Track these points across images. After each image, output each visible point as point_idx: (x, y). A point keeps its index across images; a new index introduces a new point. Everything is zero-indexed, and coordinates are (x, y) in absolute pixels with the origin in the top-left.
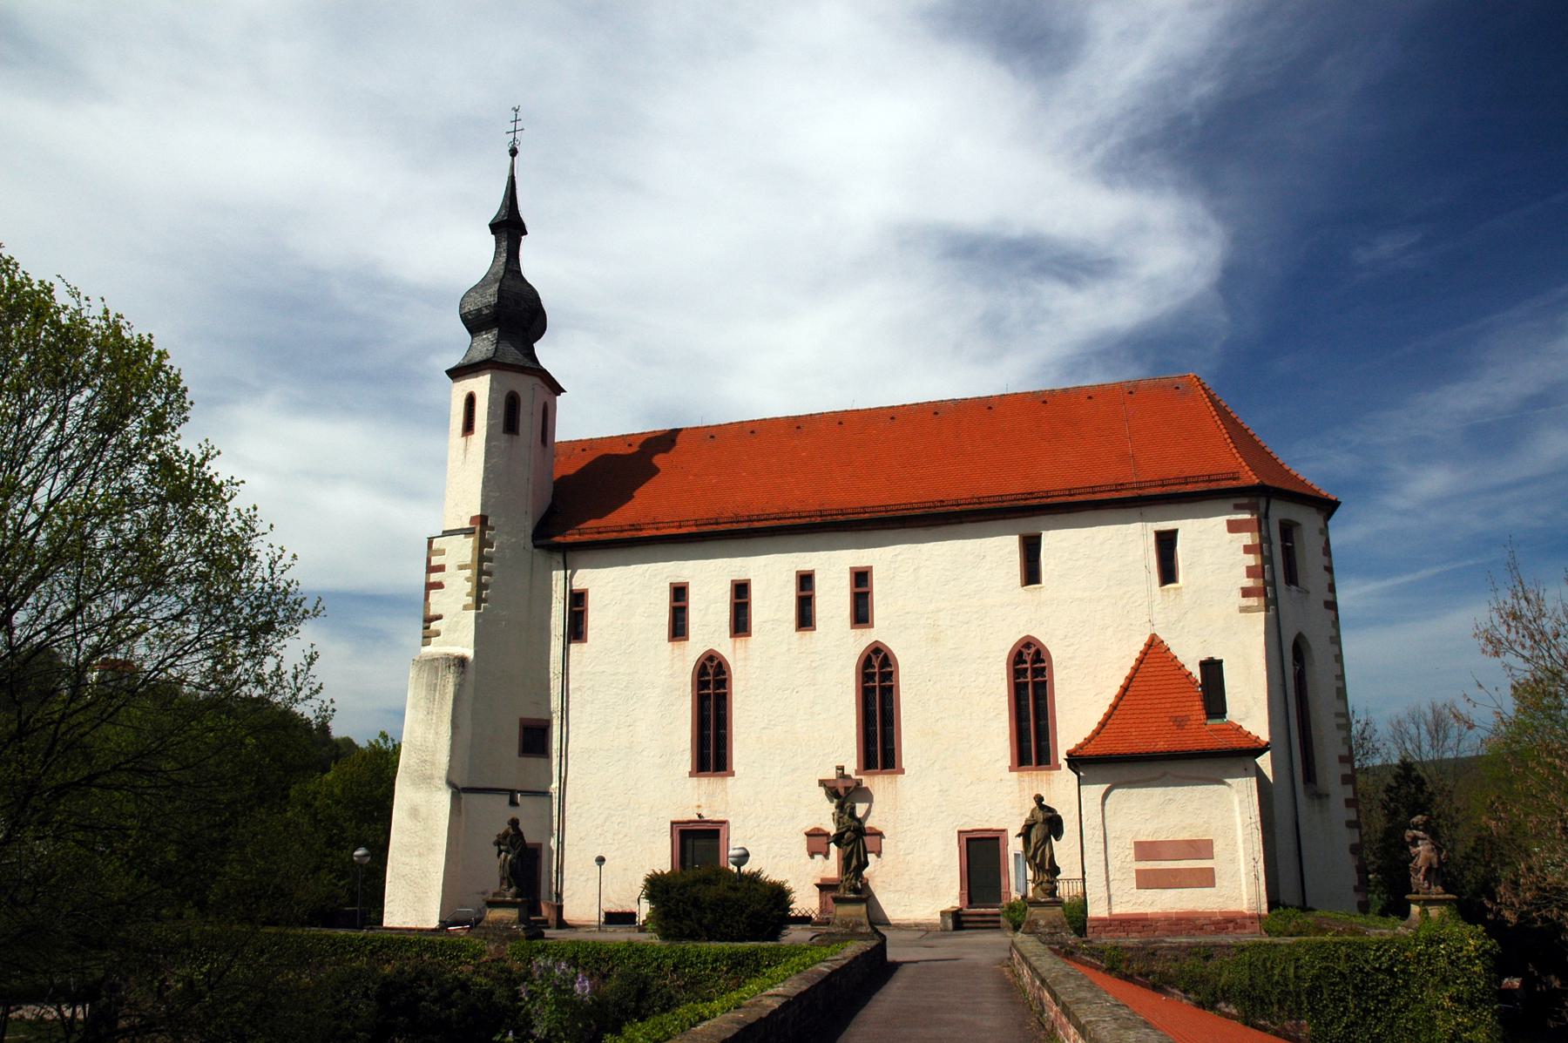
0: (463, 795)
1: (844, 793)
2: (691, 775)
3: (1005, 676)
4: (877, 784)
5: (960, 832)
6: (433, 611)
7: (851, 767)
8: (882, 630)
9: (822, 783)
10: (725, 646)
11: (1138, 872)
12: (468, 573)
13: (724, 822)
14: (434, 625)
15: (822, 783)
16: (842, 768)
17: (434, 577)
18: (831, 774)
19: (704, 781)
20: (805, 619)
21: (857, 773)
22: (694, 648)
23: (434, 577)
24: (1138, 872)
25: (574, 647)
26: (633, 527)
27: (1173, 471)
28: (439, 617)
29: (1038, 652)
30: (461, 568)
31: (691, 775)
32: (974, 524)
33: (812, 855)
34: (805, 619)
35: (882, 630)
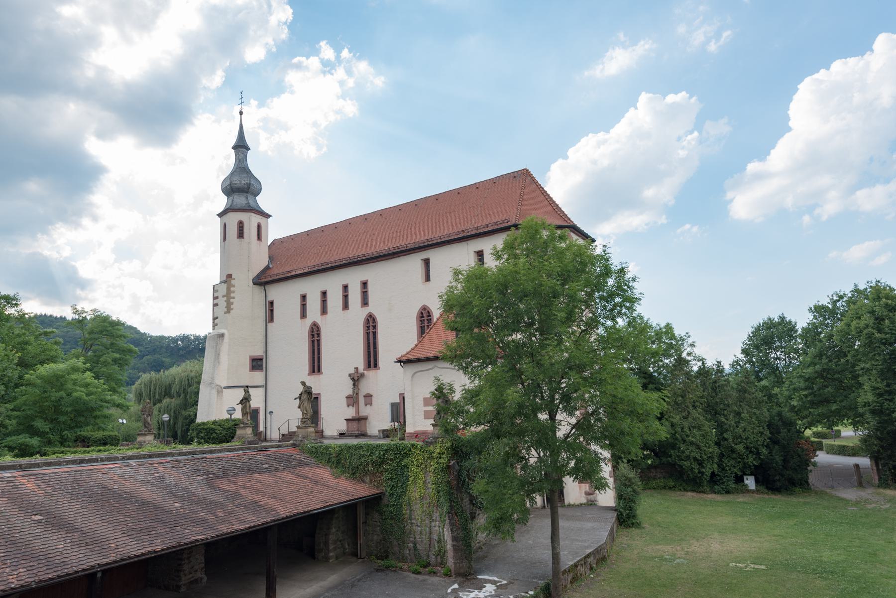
0: (224, 390)
1: (356, 379)
2: (309, 375)
3: (416, 324)
4: (370, 374)
5: (400, 394)
6: (215, 316)
7: (361, 369)
8: (371, 309)
9: (350, 375)
10: (319, 319)
11: (425, 411)
12: (225, 298)
13: (319, 394)
14: (216, 321)
15: (350, 375)
16: (357, 369)
17: (216, 301)
18: (353, 371)
19: (313, 376)
20: (346, 306)
21: (364, 370)
22: (308, 322)
23: (216, 301)
24: (425, 411)
25: (269, 325)
26: (289, 272)
27: (487, 221)
28: (217, 318)
29: (429, 312)
30: (223, 297)
31: (309, 375)
32: (405, 256)
33: (348, 406)
34: (346, 306)
35: (371, 309)
